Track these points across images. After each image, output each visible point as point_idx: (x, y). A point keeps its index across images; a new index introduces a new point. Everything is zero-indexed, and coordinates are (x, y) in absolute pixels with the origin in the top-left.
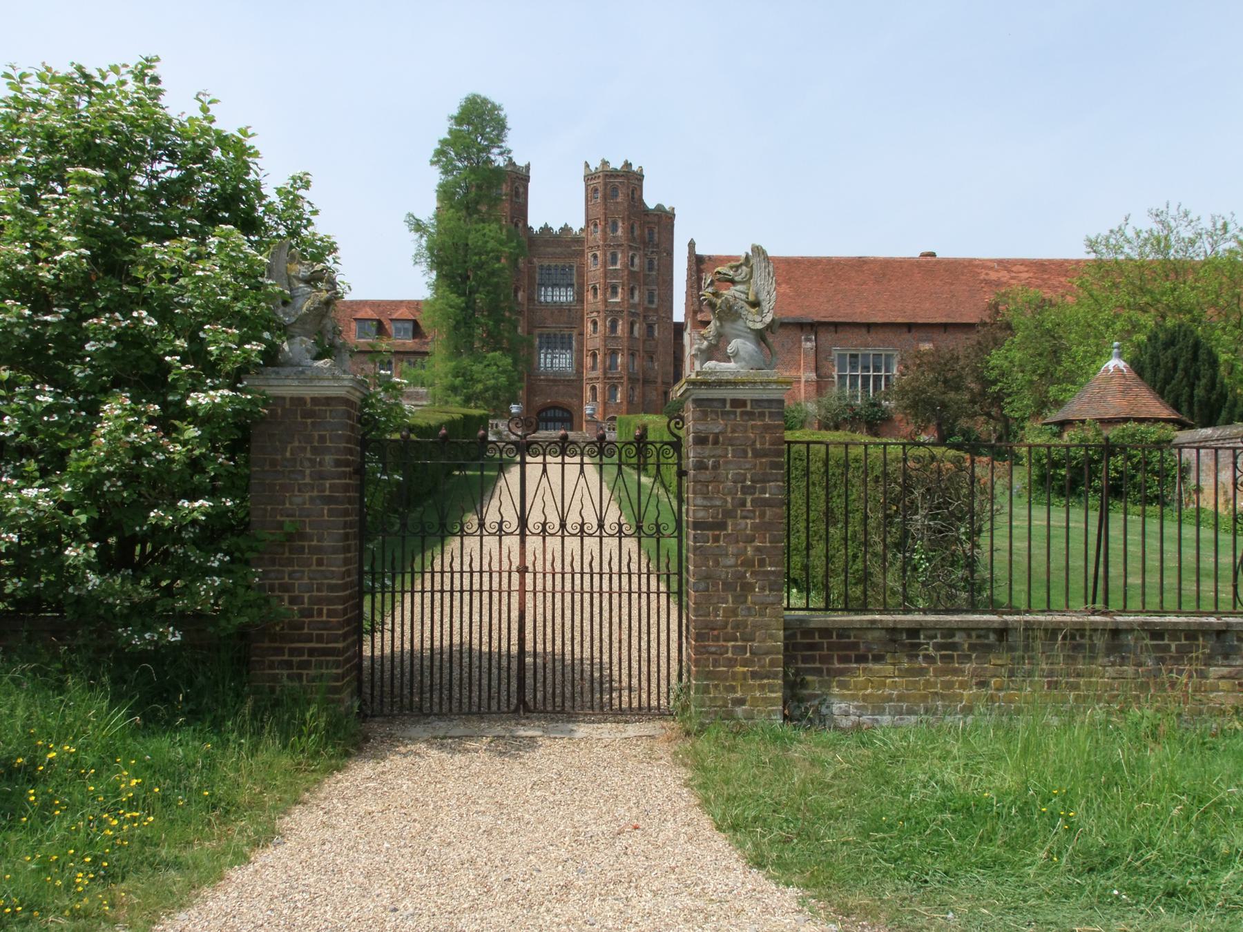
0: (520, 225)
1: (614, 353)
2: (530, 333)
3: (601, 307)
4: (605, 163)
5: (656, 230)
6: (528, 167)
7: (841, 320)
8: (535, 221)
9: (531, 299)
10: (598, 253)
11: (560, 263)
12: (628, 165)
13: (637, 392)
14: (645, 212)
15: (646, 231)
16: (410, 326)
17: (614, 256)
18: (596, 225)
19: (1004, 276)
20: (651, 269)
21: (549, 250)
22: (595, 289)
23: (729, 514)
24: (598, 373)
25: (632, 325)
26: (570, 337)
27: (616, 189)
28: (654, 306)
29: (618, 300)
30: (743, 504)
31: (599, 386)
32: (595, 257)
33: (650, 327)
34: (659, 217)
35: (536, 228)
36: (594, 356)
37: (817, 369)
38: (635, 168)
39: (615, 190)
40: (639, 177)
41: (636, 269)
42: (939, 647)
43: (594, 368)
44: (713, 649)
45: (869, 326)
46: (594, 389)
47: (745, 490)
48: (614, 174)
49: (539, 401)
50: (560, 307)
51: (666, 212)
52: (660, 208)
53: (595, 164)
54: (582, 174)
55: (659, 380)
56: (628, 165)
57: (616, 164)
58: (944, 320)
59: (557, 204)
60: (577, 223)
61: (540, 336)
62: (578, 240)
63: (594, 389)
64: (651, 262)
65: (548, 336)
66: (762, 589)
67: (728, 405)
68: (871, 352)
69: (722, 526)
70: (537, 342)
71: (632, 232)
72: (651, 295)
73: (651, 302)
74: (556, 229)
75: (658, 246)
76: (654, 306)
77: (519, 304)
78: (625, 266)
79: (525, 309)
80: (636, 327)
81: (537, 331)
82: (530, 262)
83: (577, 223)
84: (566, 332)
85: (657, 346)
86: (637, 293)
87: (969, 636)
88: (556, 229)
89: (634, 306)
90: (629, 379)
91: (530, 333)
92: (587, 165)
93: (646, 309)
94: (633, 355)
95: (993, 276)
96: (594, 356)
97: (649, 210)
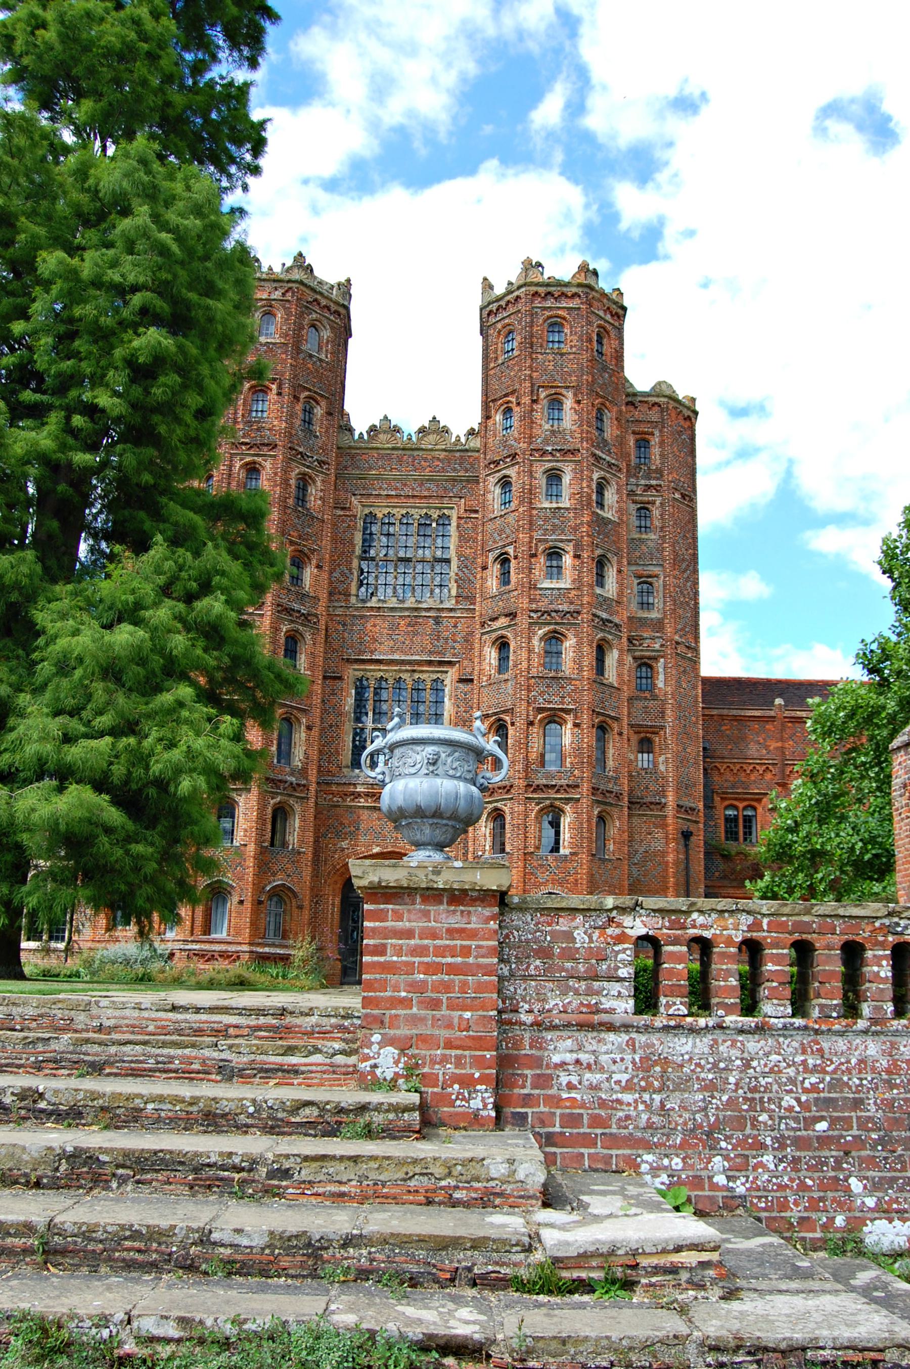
2: (332, 678)
6: (346, 287)
8: (362, 410)
9: (338, 592)
10: (512, 472)
13: (615, 828)
14: (633, 399)
17: (554, 477)
18: (508, 411)
22: (504, 560)
25: (601, 651)
26: (437, 688)
27: (556, 330)
28: (654, 615)
29: (565, 583)
32: (505, 483)
33: (645, 664)
51: (673, 399)
55: (671, 799)
60: (462, 414)
62: (459, 454)
77: (302, 597)
78: (583, 502)
79: (321, 609)
80: (612, 658)
81: (351, 673)
83: (462, 414)
86: (611, 575)
91: (332, 678)
92: (487, 285)
97: (635, 394)
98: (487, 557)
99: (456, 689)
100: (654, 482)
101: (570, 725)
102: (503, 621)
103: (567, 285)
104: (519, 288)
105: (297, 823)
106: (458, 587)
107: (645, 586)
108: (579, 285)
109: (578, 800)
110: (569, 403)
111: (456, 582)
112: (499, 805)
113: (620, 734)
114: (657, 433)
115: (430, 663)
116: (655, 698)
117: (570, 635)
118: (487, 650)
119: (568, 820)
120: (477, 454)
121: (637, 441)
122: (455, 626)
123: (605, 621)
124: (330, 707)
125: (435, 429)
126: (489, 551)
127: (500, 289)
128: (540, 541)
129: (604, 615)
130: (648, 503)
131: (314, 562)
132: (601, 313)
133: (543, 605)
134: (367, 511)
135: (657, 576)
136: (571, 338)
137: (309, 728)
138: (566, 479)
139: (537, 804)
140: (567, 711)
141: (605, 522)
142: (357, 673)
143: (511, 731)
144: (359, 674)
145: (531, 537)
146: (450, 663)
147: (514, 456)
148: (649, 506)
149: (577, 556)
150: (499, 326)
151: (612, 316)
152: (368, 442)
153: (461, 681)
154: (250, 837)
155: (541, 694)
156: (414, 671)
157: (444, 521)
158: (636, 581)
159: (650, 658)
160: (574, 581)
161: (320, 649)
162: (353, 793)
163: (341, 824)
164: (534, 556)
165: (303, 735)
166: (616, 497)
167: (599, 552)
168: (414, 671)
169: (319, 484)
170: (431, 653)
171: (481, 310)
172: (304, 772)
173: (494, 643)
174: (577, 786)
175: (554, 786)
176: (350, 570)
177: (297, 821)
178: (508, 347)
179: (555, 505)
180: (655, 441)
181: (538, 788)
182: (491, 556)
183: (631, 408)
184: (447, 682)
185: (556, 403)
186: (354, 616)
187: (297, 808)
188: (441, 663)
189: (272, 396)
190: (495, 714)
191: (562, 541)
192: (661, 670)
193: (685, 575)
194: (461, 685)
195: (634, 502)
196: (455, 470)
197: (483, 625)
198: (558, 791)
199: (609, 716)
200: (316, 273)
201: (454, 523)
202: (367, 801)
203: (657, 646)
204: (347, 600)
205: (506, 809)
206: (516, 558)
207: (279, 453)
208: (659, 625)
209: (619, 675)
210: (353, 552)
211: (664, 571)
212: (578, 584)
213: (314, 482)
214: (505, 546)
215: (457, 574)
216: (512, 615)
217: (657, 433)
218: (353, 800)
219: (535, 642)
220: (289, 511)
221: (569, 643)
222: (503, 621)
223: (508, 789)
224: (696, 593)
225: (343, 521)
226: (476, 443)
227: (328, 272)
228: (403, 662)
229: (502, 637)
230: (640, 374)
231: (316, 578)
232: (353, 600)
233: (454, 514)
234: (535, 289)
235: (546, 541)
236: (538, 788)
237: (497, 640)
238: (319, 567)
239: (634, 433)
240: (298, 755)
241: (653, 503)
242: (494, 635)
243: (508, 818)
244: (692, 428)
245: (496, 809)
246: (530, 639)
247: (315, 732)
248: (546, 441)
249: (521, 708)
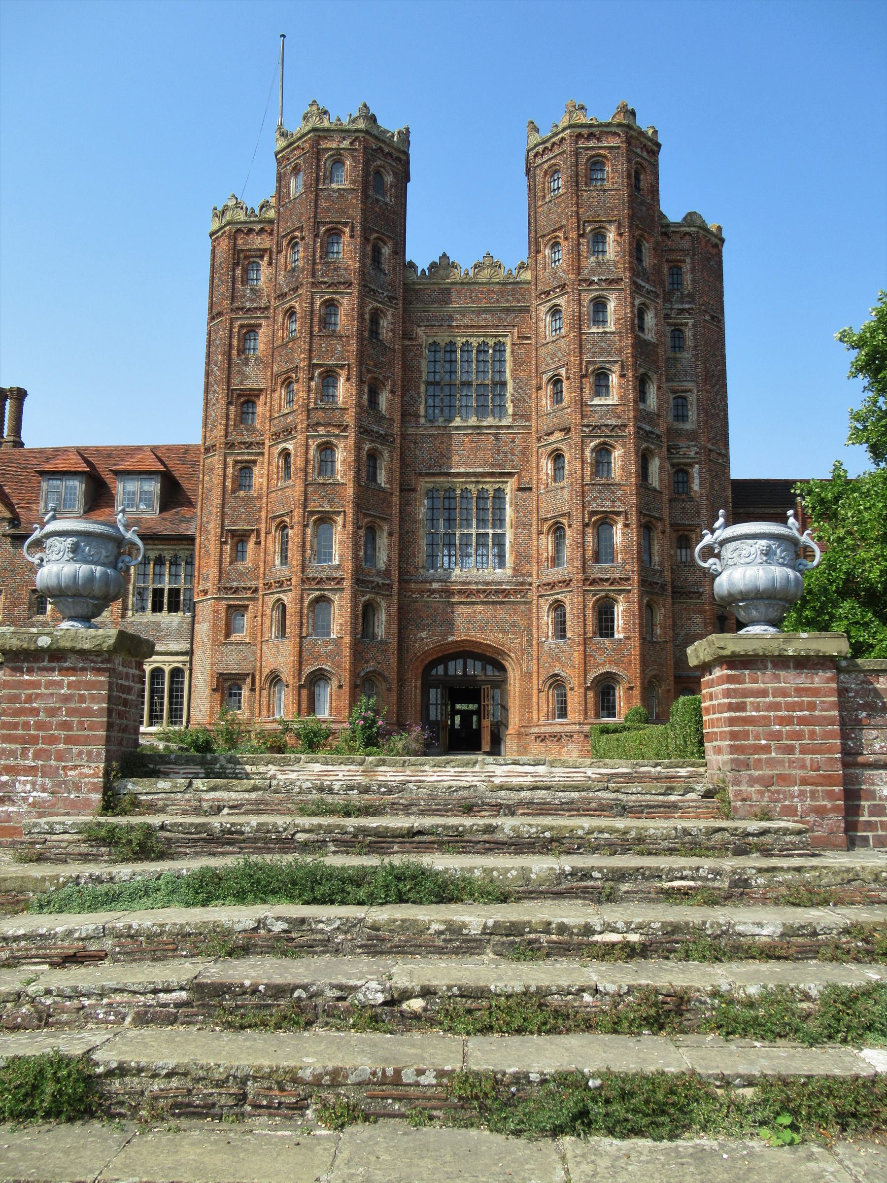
0: (386, 251)
1: (604, 522)
2: (406, 489)
3: (575, 419)
6: (405, 136)
10: (562, 301)
14: (666, 229)
16: (153, 487)
17: (599, 305)
22: (556, 381)
24: (569, 568)
26: (499, 496)
29: (613, 399)
31: (571, 601)
32: (555, 311)
35: (423, 264)
36: (558, 530)
38: (643, 123)
39: (596, 164)
43: (556, 560)
46: (558, 606)
49: (426, 639)
51: (704, 228)
59: (465, 218)
61: (431, 494)
62: (511, 285)
63: (558, 606)
64: (677, 332)
71: (640, 260)
73: (681, 417)
77: (380, 418)
79: (396, 429)
80: (655, 465)
81: (425, 484)
82: (407, 335)
90: (643, 582)
91: (406, 489)
96: (558, 530)
97: (668, 225)
98: (541, 379)
99: (516, 496)
100: (687, 306)
101: (620, 526)
102: (558, 435)
103: (609, 125)
104: (564, 130)
105: (383, 617)
106: (514, 406)
107: (680, 401)
108: (619, 125)
109: (629, 591)
110: (611, 236)
111: (512, 401)
112: (559, 597)
113: (663, 532)
114: (688, 260)
115: (492, 474)
116: (691, 499)
117: (618, 446)
118: (543, 461)
119: (621, 608)
120: (527, 286)
121: (670, 268)
122: (513, 441)
123: (648, 433)
124: (405, 515)
125: (490, 263)
126: (543, 373)
128: (588, 363)
129: (648, 428)
130: (682, 325)
131: (388, 388)
132: (638, 151)
133: (593, 421)
134: (431, 341)
135: (690, 391)
136: (613, 175)
137: (390, 534)
138: (611, 306)
139: (594, 595)
140: (618, 514)
141: (646, 343)
142: (428, 485)
143: (568, 532)
144: (430, 486)
145: (581, 360)
146: (510, 475)
147: (563, 286)
148: (683, 328)
149: (622, 376)
150: (546, 166)
151: (648, 153)
152: (429, 278)
153: (520, 489)
154: (346, 631)
155: (595, 499)
156: (478, 482)
158: (672, 396)
159: (686, 464)
160: (621, 399)
161: (397, 465)
162: (429, 590)
163: (420, 617)
164: (585, 376)
165: (386, 540)
166: (654, 321)
167: (642, 371)
168: (478, 482)
169: (389, 317)
170: (493, 465)
171: (528, 152)
172: (387, 573)
173: (549, 456)
174: (628, 579)
175: (607, 580)
176: (419, 394)
177: (384, 615)
178: (554, 185)
179: (601, 330)
180: (687, 267)
181: (594, 582)
182: (545, 378)
183: (665, 238)
184: (508, 490)
185: (599, 237)
186: (423, 435)
187: (383, 604)
188: (502, 474)
189: (346, 238)
190: (554, 517)
191: (609, 362)
192: (696, 475)
193: (715, 389)
194: (519, 493)
195: (669, 324)
196: (508, 301)
197: (539, 439)
198: (612, 584)
199: (653, 517)
200: (379, 123)
201: (508, 350)
202: (441, 597)
203: (692, 454)
204: (417, 422)
205: (567, 601)
206: (568, 378)
207: (355, 290)
208: (693, 436)
209: (661, 481)
210: (421, 377)
211: (698, 386)
213: (385, 315)
214: (557, 368)
215: (513, 395)
216: (567, 430)
217: (688, 260)
218: (429, 596)
219: (588, 453)
220: (365, 342)
221: (617, 454)
222: (558, 435)
223: (567, 583)
224: (726, 405)
225: (411, 351)
226: (527, 276)
227: (390, 123)
228: (467, 475)
229: (557, 450)
230: (673, 208)
231: (390, 402)
232: (422, 421)
233: (508, 341)
234: (578, 130)
235: (594, 362)
236: (594, 582)
237: (552, 452)
238: (392, 392)
239: (668, 261)
240: (382, 558)
241: (686, 324)
242: (550, 449)
243: (568, 608)
244: (719, 255)
245: (557, 601)
246: (583, 450)
247: (395, 538)
248: (593, 272)
249: (577, 512)
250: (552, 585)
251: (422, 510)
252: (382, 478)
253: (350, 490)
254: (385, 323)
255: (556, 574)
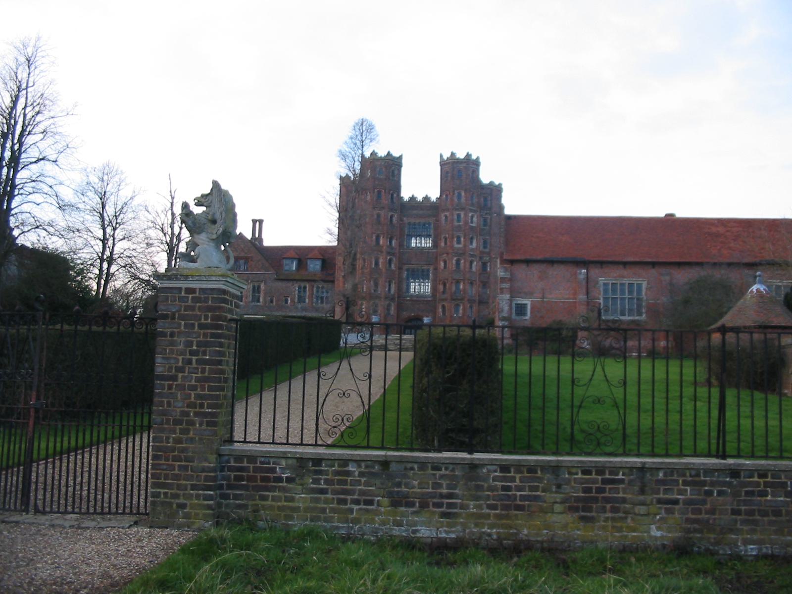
0: (395, 195)
2: (400, 269)
4: (453, 154)
5: (489, 198)
6: (400, 157)
7: (605, 259)
11: (422, 221)
12: (468, 156)
15: (482, 199)
19: (721, 230)
20: (485, 225)
21: (415, 212)
22: (446, 239)
23: (180, 370)
25: (471, 262)
26: (428, 271)
28: (487, 250)
29: (460, 246)
30: (190, 362)
33: (484, 265)
34: (491, 190)
37: (587, 293)
38: (474, 157)
40: (477, 163)
41: (474, 225)
42: (338, 473)
43: (444, 292)
44: (165, 467)
45: (625, 264)
46: (444, 307)
47: (192, 353)
48: (458, 162)
49: (405, 314)
50: (420, 250)
52: (491, 183)
53: (446, 156)
54: (439, 161)
56: (468, 156)
57: (461, 155)
58: (678, 260)
59: (420, 183)
60: (434, 193)
61: (408, 270)
64: (485, 220)
65: (413, 270)
66: (201, 425)
67: (183, 292)
68: (626, 281)
69: (174, 378)
70: (405, 274)
72: (485, 242)
74: (420, 198)
75: (490, 209)
76: (487, 250)
77: (392, 248)
78: (466, 223)
79: (397, 251)
81: (406, 267)
83: (434, 193)
84: (425, 267)
85: (489, 278)
87: (360, 466)
88: (420, 198)
89: (472, 250)
91: (400, 269)
92: (441, 156)
93: (482, 252)
94: (472, 283)
95: (714, 229)
125: (426, 198)
127: (445, 158)
157: (429, 224)
172: (394, 295)
187: (393, 304)
212: (465, 246)
216: (448, 254)
222: (445, 255)
227: (396, 154)
240: (392, 291)
250: (443, 300)
251: (405, 274)
252: (393, 266)
253: (384, 270)
254: (394, 219)
255: (444, 297)
